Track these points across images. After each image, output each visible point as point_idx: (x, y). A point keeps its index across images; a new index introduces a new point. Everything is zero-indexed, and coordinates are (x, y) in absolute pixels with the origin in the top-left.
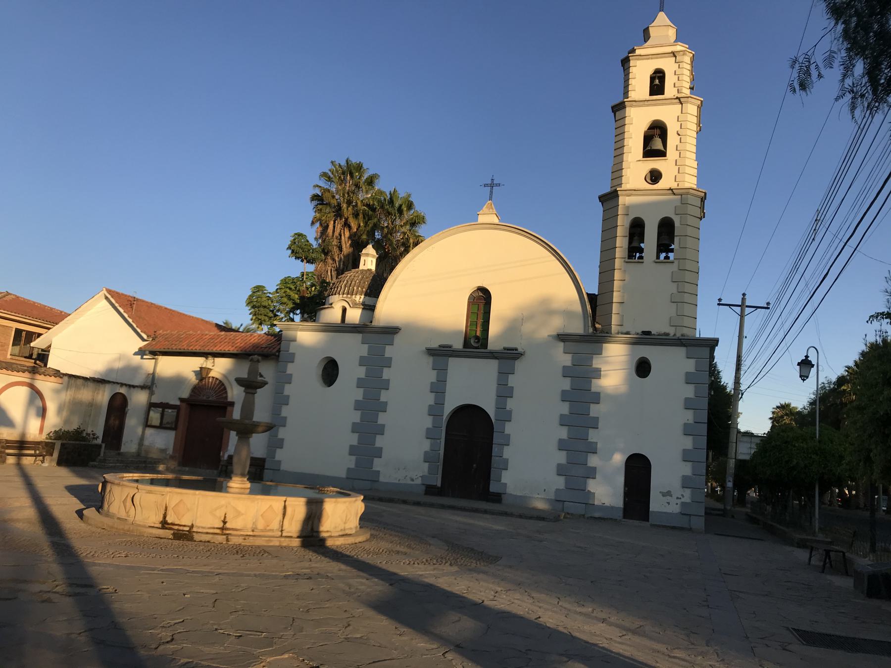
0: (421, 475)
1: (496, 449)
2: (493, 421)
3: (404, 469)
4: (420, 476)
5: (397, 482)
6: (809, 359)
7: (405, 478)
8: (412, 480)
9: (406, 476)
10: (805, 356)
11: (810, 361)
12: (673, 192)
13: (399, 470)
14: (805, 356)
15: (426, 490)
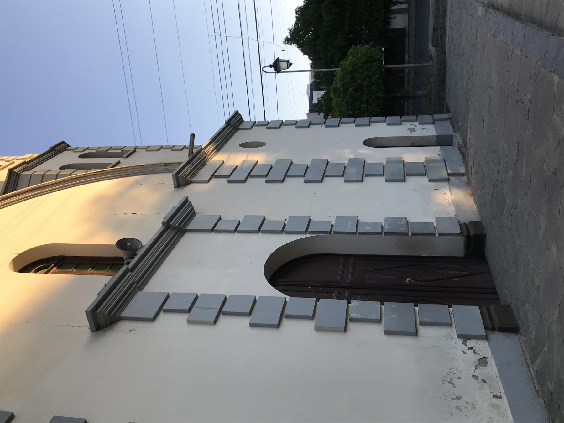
0: (460, 342)
1: (370, 228)
2: (308, 235)
3: (451, 382)
4: (464, 343)
5: (504, 404)
6: (272, 64)
7: (484, 381)
8: (483, 362)
9: (476, 377)
10: (271, 67)
11: (273, 63)
12: (56, 150)
13: (459, 398)
14: (271, 67)
15: (503, 330)
